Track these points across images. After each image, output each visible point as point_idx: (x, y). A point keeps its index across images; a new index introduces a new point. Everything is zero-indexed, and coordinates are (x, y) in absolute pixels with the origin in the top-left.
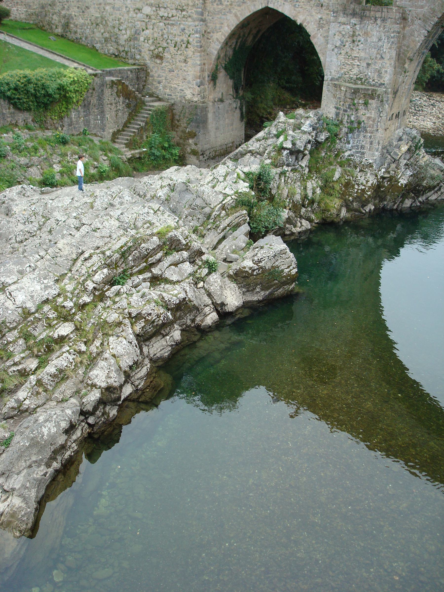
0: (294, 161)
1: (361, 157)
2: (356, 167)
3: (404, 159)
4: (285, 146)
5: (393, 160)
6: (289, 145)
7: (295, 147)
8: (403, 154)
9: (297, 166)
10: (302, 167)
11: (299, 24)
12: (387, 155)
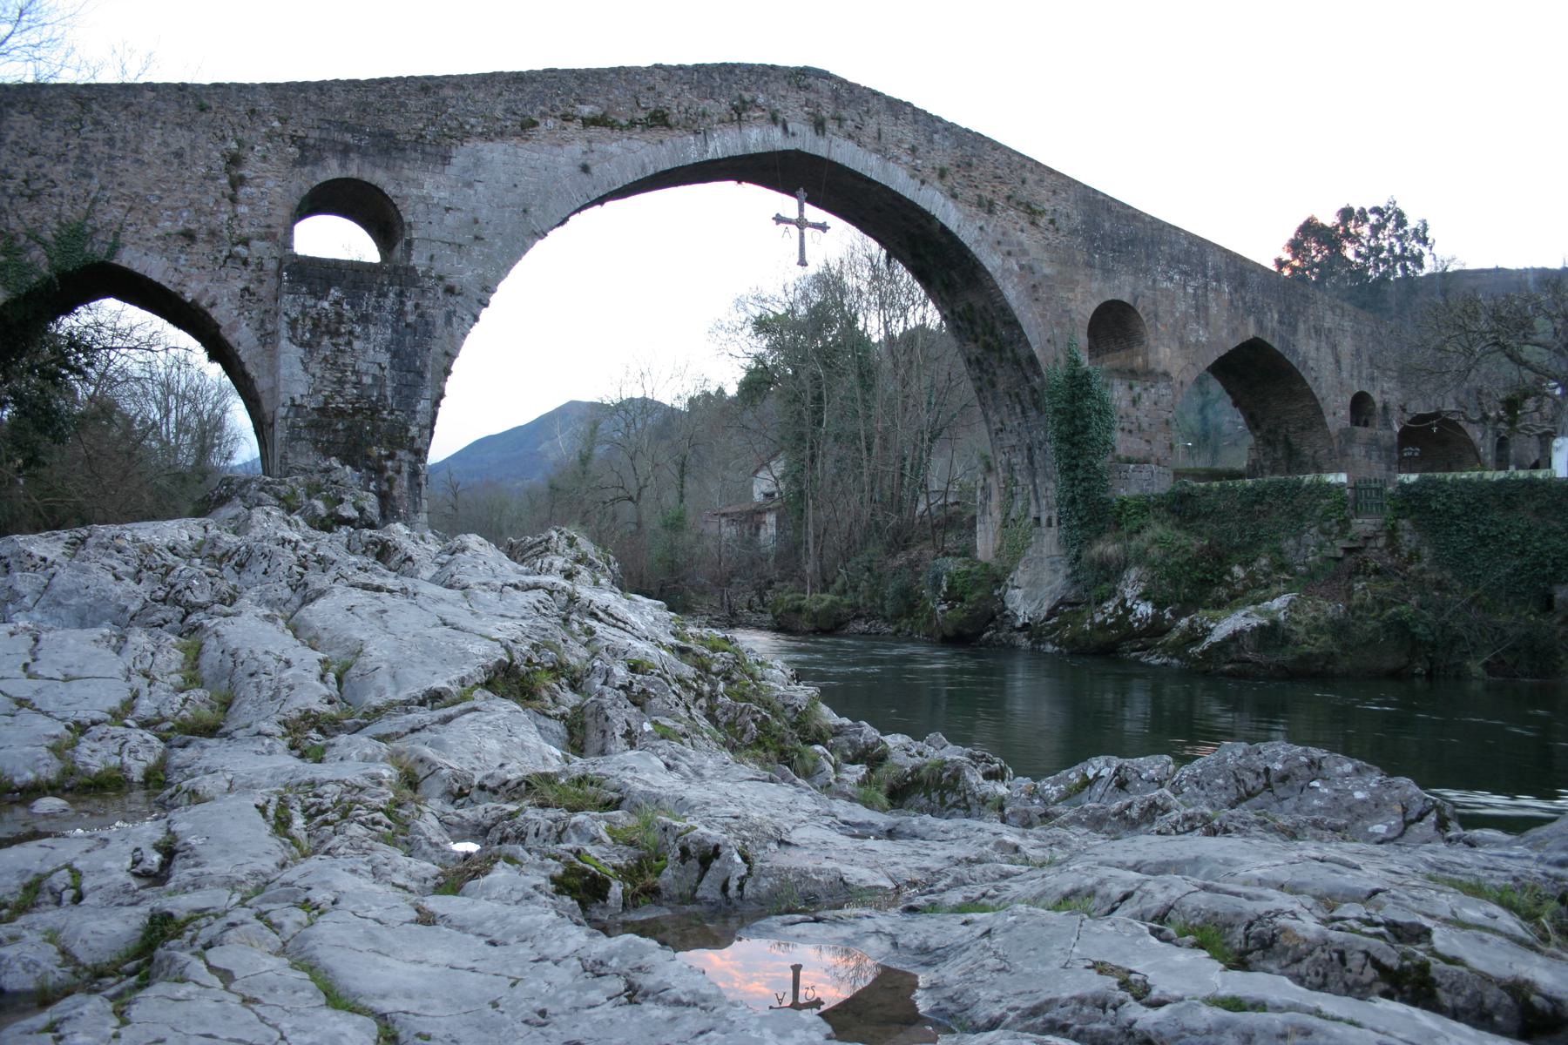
4: (344, 514)
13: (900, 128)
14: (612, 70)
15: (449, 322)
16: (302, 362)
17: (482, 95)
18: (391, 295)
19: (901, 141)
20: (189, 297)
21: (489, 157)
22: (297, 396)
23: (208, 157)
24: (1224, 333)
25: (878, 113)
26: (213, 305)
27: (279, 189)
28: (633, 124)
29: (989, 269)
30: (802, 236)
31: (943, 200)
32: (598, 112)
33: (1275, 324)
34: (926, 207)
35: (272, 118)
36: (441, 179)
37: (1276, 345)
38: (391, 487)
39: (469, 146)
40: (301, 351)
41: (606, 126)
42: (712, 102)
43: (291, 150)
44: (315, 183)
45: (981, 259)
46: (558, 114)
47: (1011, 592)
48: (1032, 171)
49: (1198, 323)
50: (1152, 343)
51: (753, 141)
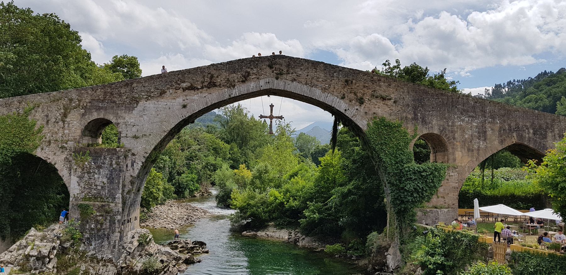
0: (41, 265)
1: (102, 255)
2: (98, 262)
3: (138, 251)
4: (31, 254)
5: (129, 253)
6: (35, 253)
7: (41, 254)
8: (136, 248)
9: (44, 269)
10: (49, 269)
11: (49, 162)
12: (123, 250)
13: (318, 73)
14: (194, 69)
15: (132, 165)
16: (78, 182)
17: (147, 84)
18: (108, 158)
19: (318, 78)
20: (49, 161)
21: (148, 106)
22: (76, 194)
23: (55, 115)
24: (496, 142)
25: (308, 69)
26: (55, 164)
27: (78, 124)
28: (202, 88)
29: (361, 126)
30: (271, 122)
31: (338, 100)
32: (189, 85)
33: (531, 135)
34: (330, 104)
35: (77, 100)
36: (132, 115)
37: (531, 146)
38: (101, 226)
39: (141, 103)
40: (78, 179)
41: (192, 89)
42: (235, 75)
43: (82, 111)
44: (89, 121)
45: (356, 122)
46: (174, 87)
47: (388, 256)
48: (384, 82)
49: (479, 139)
50: (450, 150)
51: (252, 87)
